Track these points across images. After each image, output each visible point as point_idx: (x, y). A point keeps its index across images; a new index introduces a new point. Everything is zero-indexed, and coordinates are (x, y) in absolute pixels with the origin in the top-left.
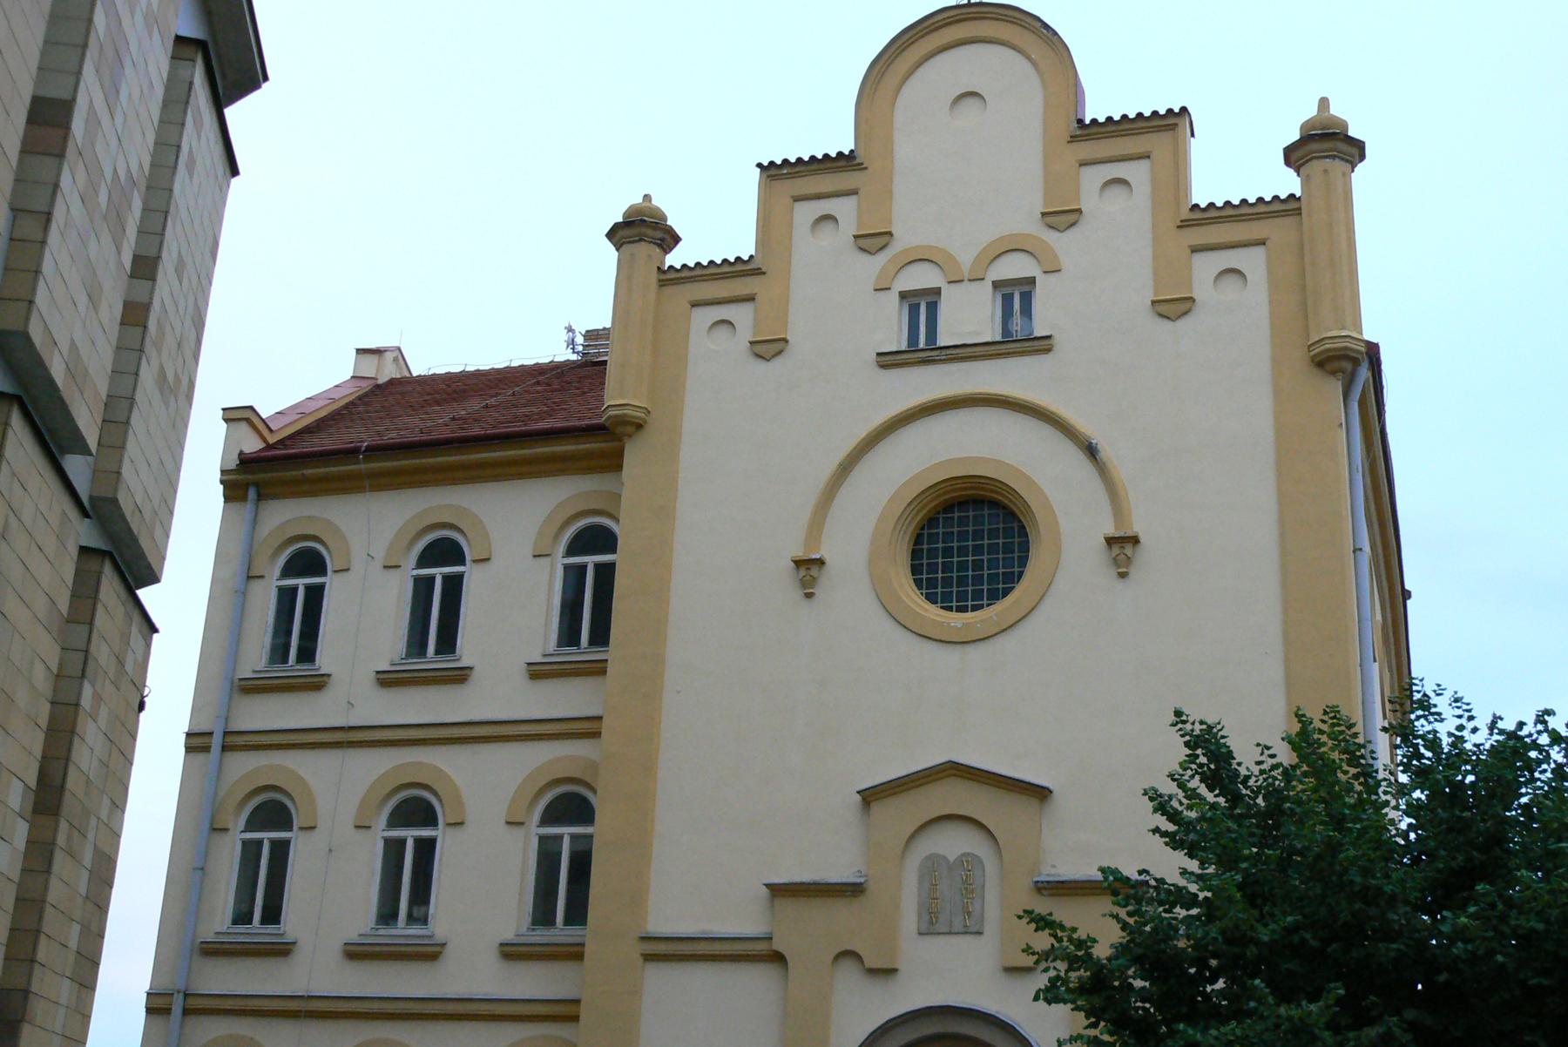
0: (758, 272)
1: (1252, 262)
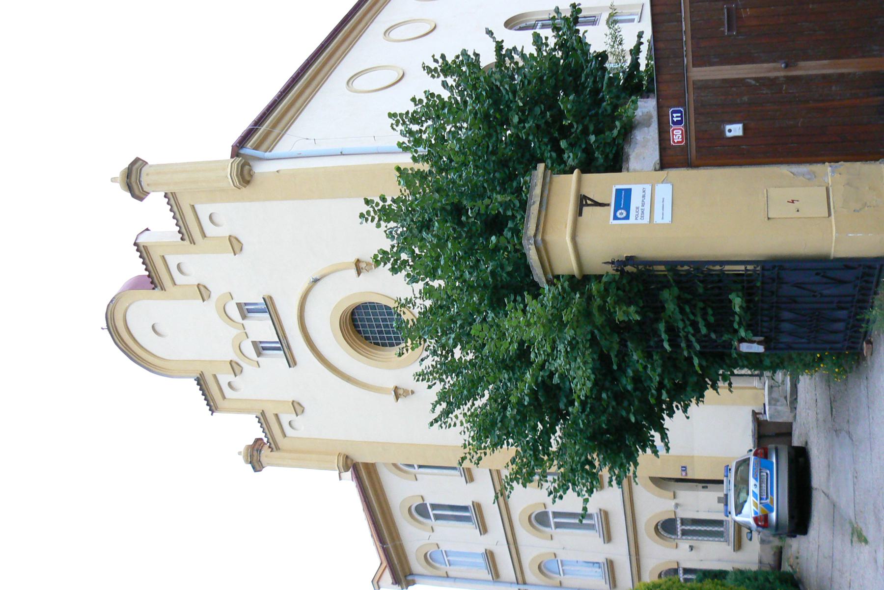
0: (263, 413)
1: (204, 211)
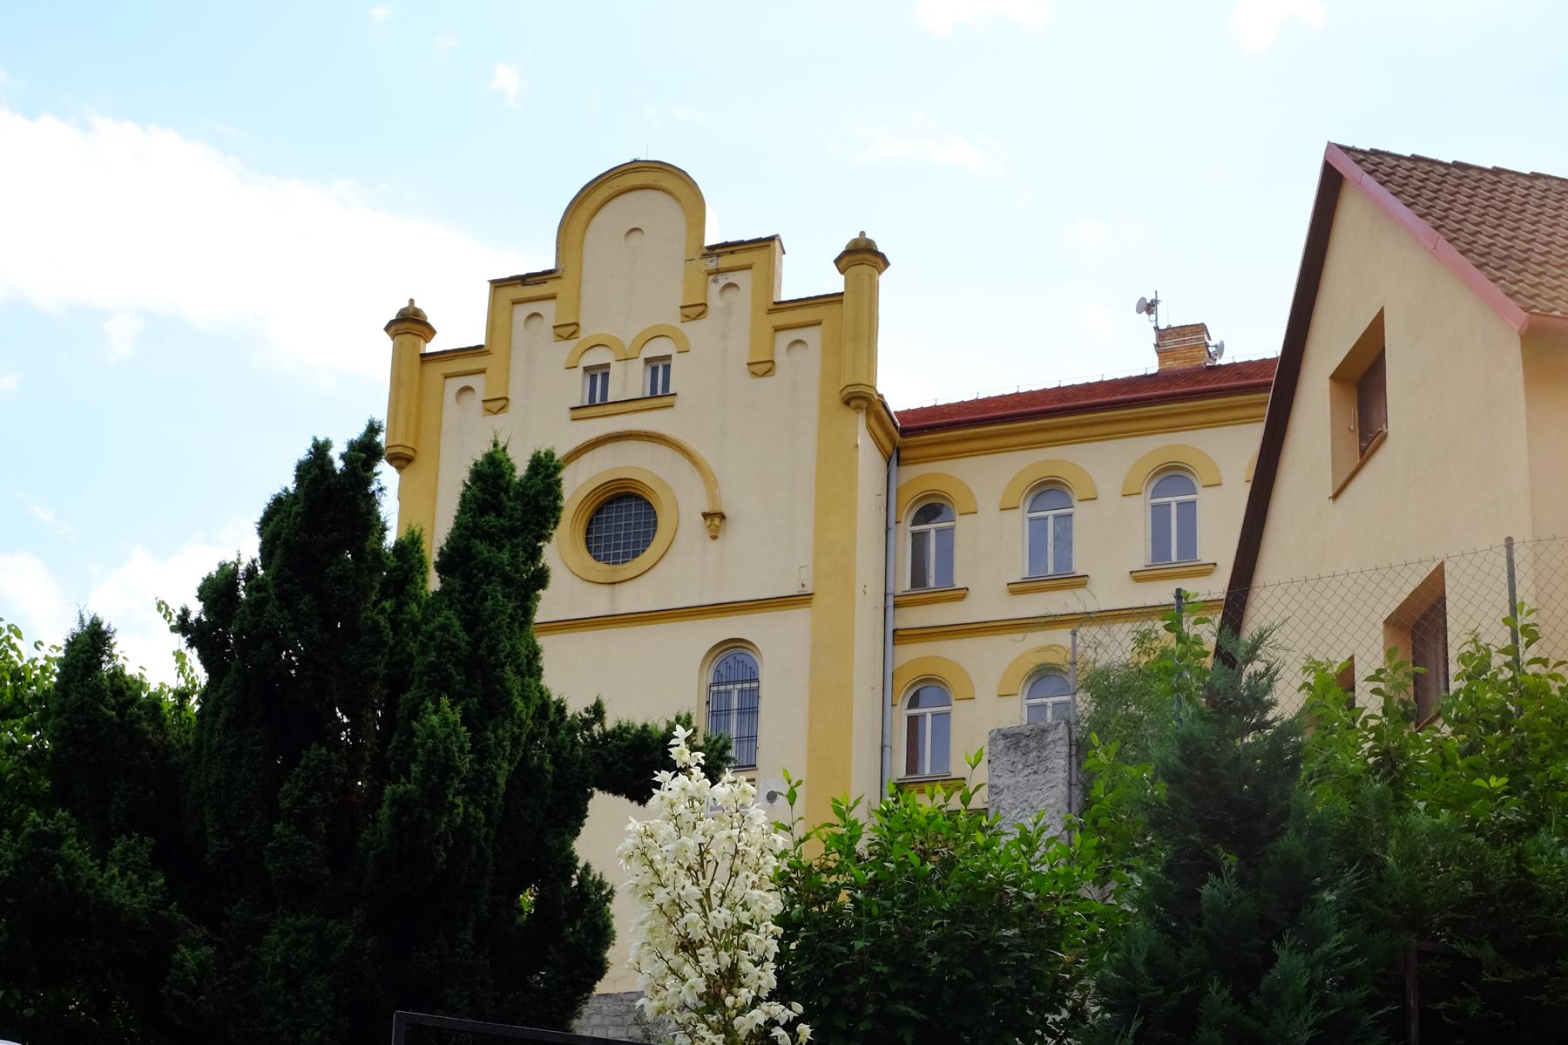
0: (487, 353)
1: (812, 336)
